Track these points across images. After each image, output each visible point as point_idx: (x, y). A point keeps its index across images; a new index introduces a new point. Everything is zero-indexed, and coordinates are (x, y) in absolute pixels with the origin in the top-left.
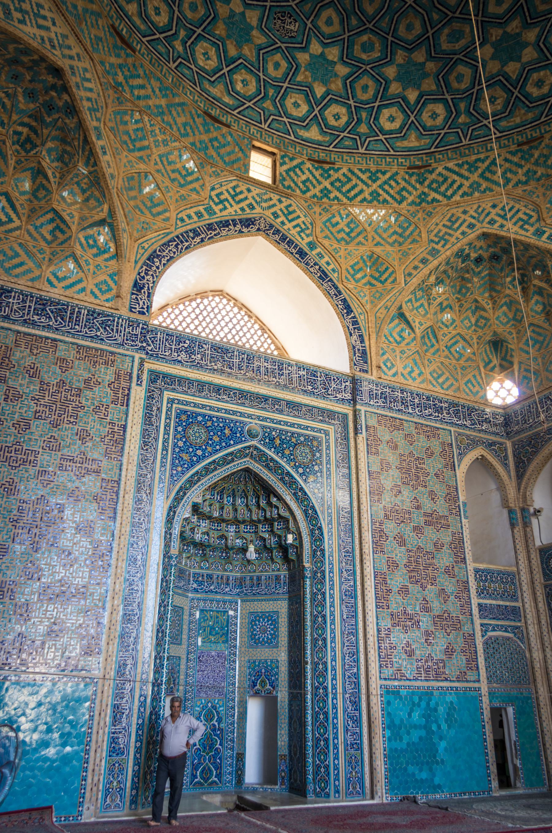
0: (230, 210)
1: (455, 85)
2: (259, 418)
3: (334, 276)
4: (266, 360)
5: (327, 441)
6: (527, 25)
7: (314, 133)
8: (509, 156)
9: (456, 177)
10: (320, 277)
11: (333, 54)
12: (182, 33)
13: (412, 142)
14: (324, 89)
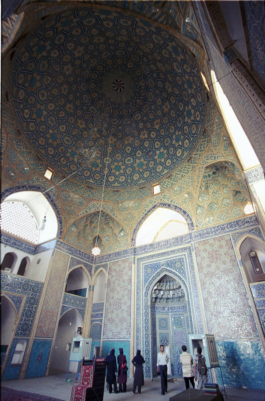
0: (150, 207)
1: (186, 132)
2: (164, 259)
3: (179, 206)
4: (163, 242)
5: (185, 257)
6: (188, 106)
7: (166, 171)
8: (203, 140)
9: (196, 156)
10: (175, 209)
11: (162, 150)
12: (129, 178)
13: (186, 154)
14: (164, 159)
